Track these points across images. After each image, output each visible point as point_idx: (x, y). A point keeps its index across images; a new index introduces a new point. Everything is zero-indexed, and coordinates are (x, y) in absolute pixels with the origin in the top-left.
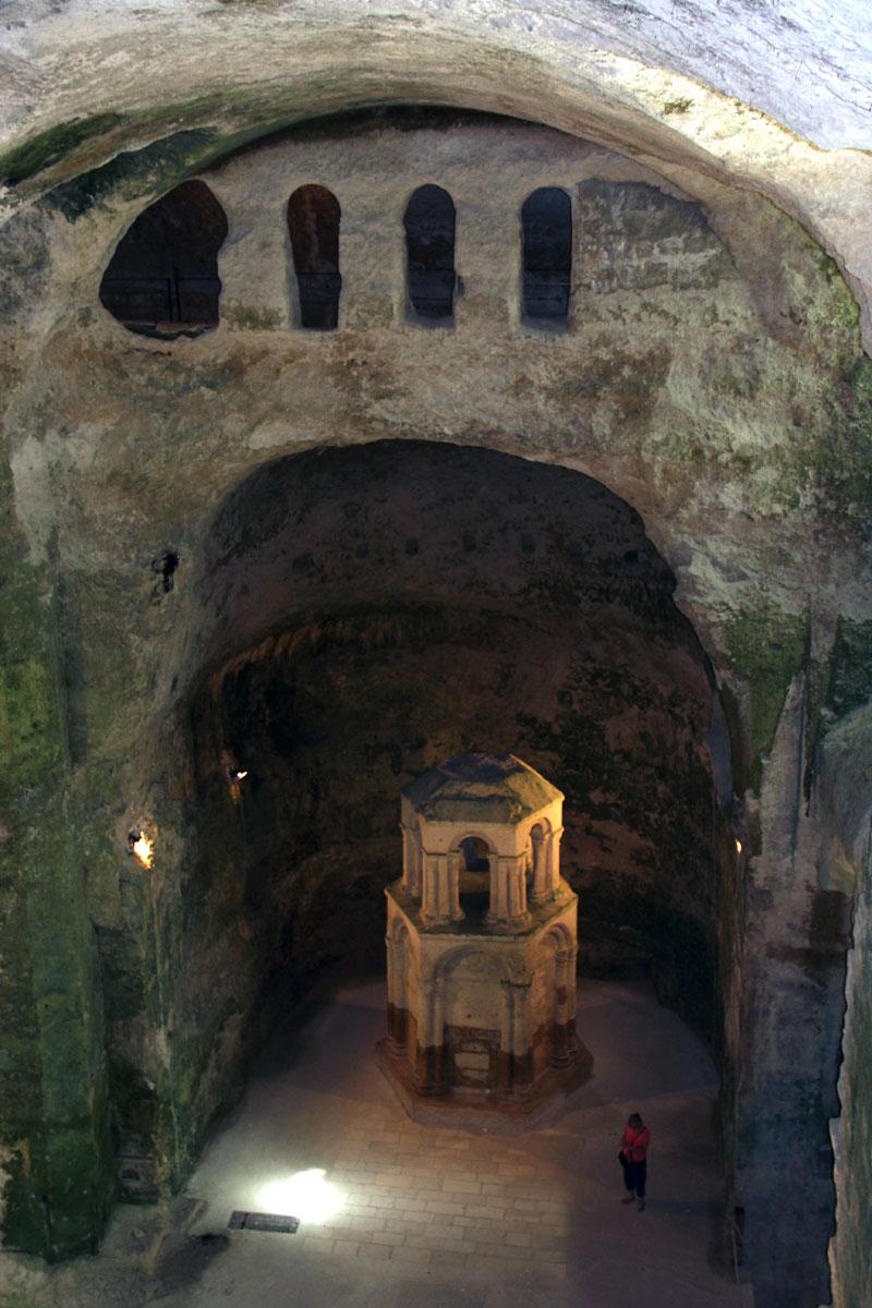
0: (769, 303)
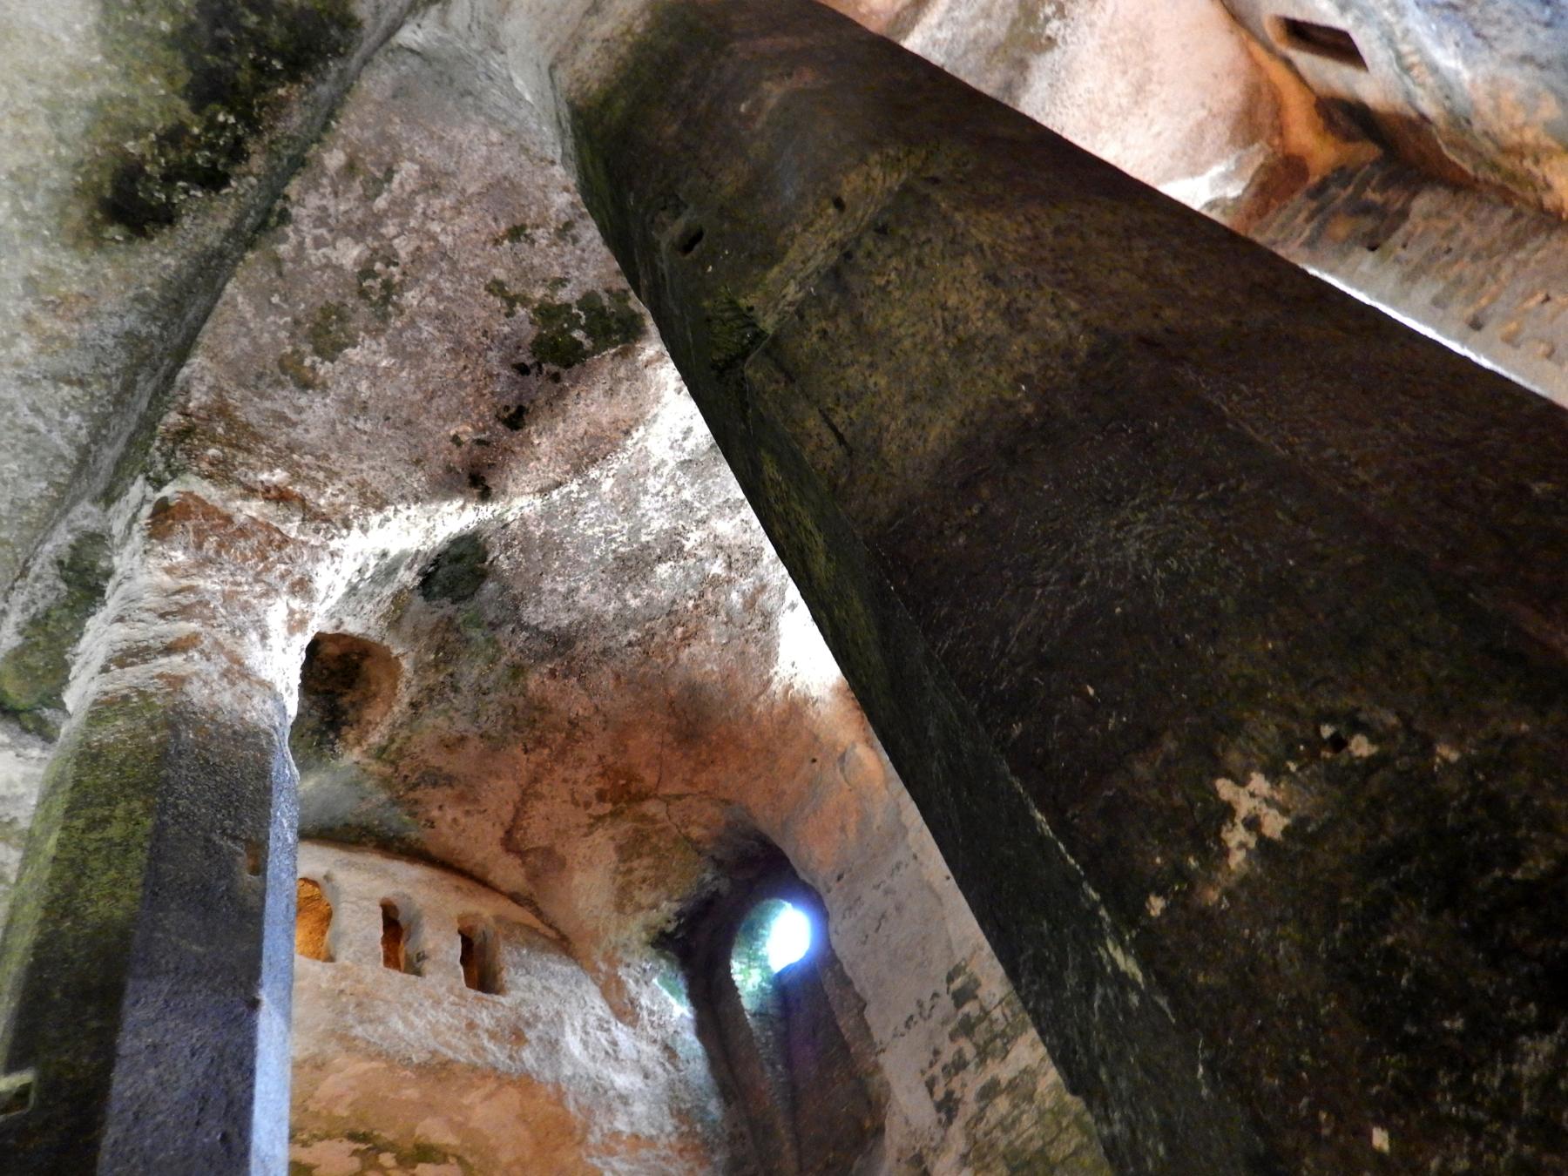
0: (615, 999)
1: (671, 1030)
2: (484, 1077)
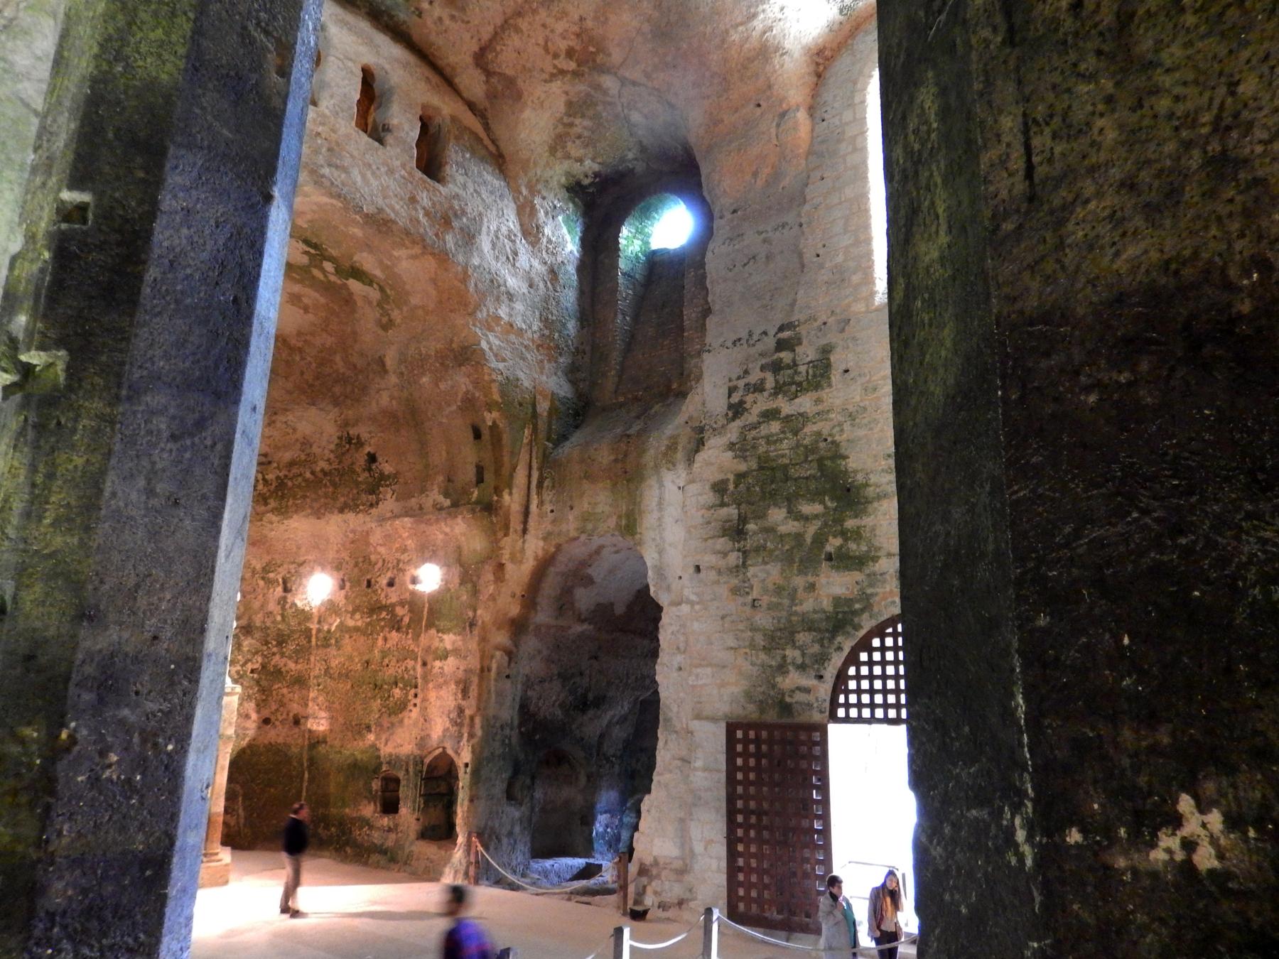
1: (560, 259)
2: (414, 242)
